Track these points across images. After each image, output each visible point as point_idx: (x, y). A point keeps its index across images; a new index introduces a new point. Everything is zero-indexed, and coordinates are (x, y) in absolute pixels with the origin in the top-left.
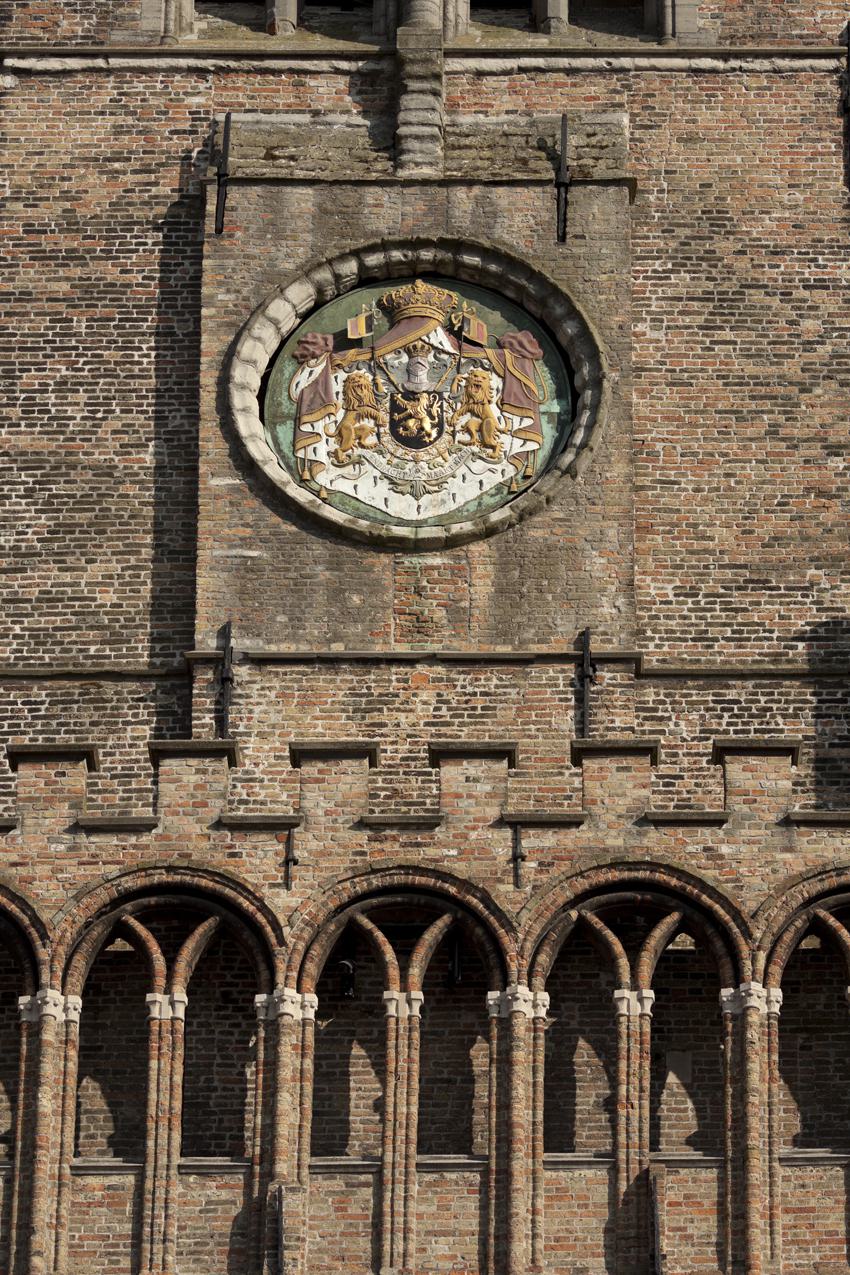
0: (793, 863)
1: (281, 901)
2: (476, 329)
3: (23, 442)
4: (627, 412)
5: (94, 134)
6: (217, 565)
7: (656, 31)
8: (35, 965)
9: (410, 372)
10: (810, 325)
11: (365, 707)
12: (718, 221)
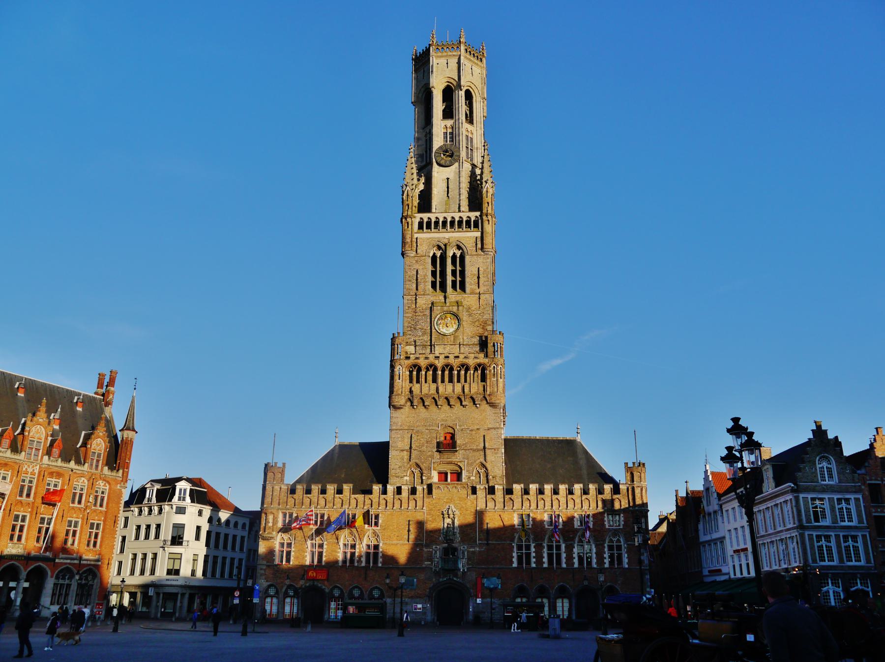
0: (474, 362)
1: (438, 365)
3: (420, 327)
5: (424, 302)
7: (465, 293)
10: (476, 317)
12: (469, 308)
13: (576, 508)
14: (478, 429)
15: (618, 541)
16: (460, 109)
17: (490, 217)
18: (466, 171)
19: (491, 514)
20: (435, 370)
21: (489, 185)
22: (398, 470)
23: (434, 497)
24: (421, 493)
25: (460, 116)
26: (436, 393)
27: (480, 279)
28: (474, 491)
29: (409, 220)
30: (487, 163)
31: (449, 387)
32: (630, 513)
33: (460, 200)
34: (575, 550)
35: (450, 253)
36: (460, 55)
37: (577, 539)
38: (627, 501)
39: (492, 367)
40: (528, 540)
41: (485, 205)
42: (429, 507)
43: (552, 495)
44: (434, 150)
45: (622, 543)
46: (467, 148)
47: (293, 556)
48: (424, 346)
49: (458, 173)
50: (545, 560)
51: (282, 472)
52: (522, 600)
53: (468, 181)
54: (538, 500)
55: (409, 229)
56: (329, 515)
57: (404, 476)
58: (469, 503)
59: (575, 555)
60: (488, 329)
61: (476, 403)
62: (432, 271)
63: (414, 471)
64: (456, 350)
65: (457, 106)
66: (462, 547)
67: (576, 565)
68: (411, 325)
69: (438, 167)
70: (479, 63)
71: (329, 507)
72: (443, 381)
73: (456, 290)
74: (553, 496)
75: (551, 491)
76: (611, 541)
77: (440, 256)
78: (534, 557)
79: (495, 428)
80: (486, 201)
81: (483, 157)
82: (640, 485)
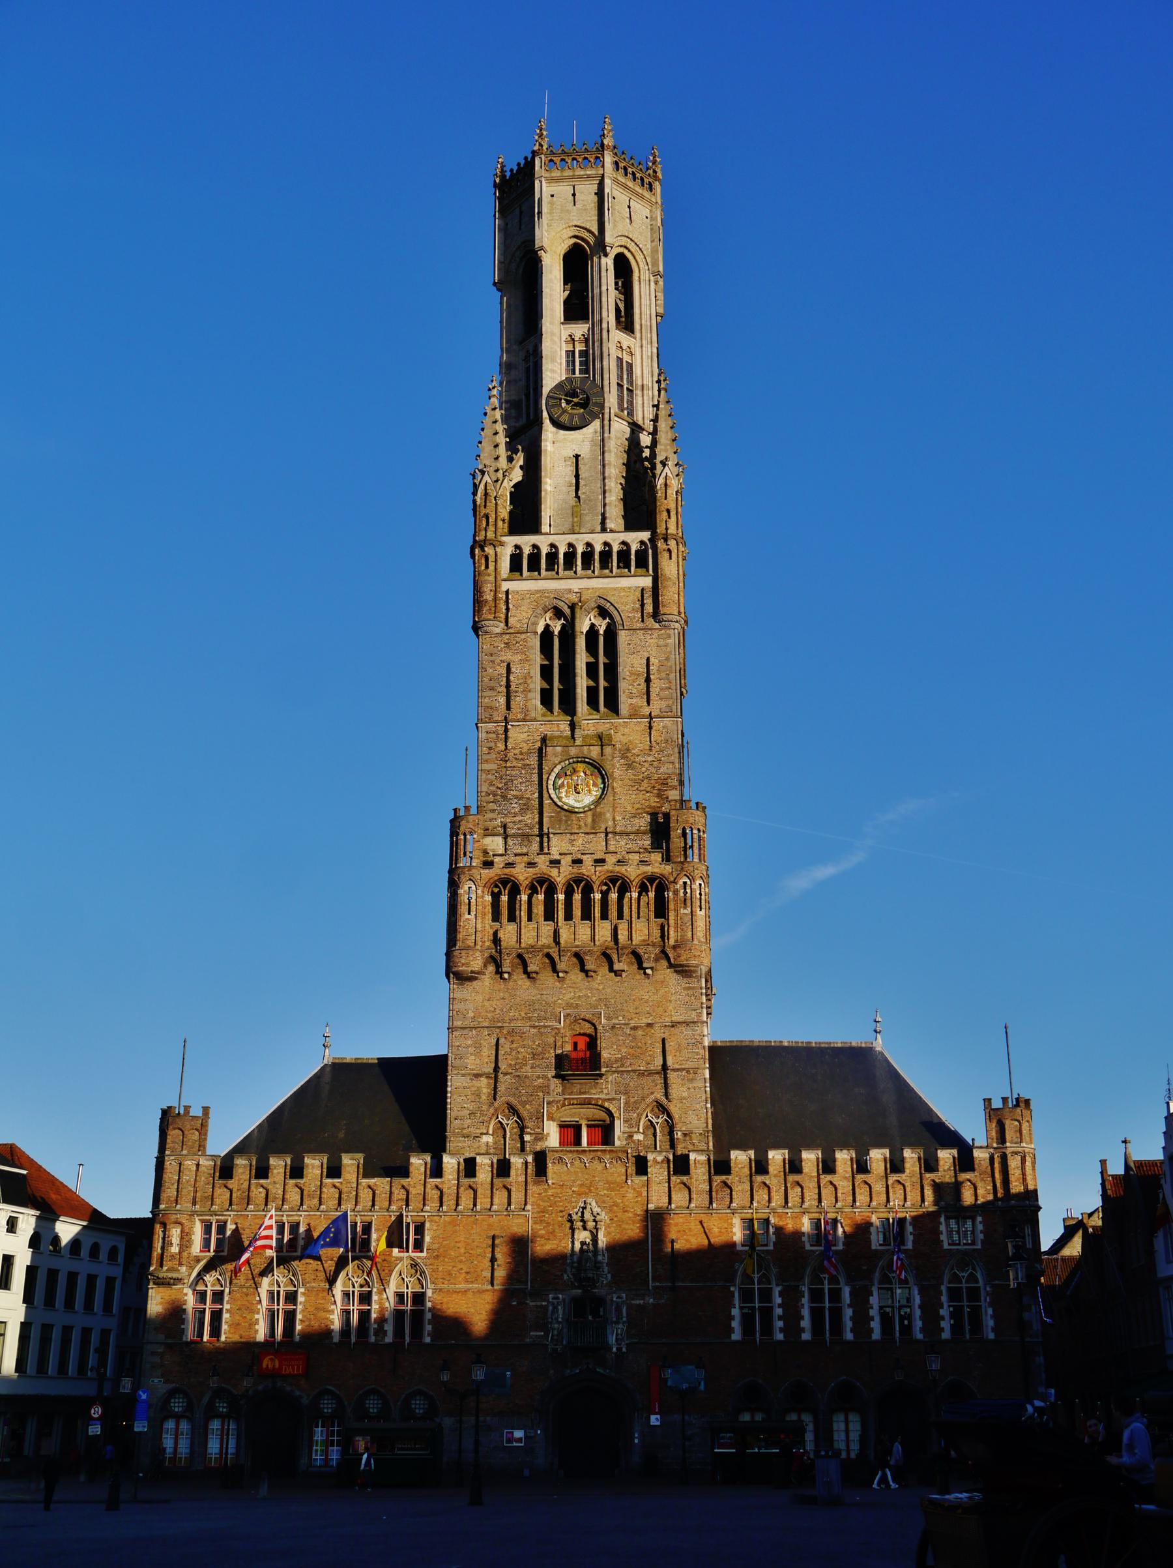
0: (639, 872)
1: (558, 879)
2: (588, 772)
3: (515, 793)
4: (613, 788)
5: (524, 736)
6: (547, 817)
8: (520, 891)
9: (577, 780)
10: (644, 769)
11: (571, 841)
12: (628, 750)
13: (874, 1204)
14: (650, 1025)
15: (972, 1278)
16: (604, 299)
17: (672, 543)
18: (617, 438)
19: (681, 1220)
20: (551, 890)
21: (670, 470)
22: (469, 1121)
23: (550, 1182)
24: (519, 1172)
25: (604, 314)
26: (554, 944)
27: (651, 684)
28: (641, 1166)
29: (489, 550)
30: (665, 421)
31: (584, 930)
33: (605, 505)
34: (874, 1300)
35: (583, 626)
36: (603, 175)
38: (990, 1187)
39: (681, 882)
40: (765, 1279)
41: (662, 516)
42: (539, 1205)
43: (819, 1175)
44: (546, 391)
45: (981, 1284)
46: (620, 386)
47: (226, 1322)
48: (525, 837)
49: (599, 443)
50: (806, 1323)
51: (203, 1129)
52: (753, 1417)
53: (622, 461)
54: (788, 1185)
55: (489, 571)
56: (309, 1225)
57: (482, 1134)
58: (630, 1195)
59: (874, 1312)
60: (670, 798)
61: (645, 965)
62: (541, 665)
63: (505, 1122)
64: (597, 845)
65: (596, 291)
67: (876, 1335)
68: (493, 788)
69: (554, 429)
70: (647, 194)
71: (311, 1209)
72: (568, 917)
73: (598, 710)
74: (822, 1177)
75: (818, 1166)
76: (955, 1278)
77: (560, 633)
78: (780, 1318)
79: (687, 1023)
80: (664, 508)
81: (657, 406)
82: (1020, 1150)
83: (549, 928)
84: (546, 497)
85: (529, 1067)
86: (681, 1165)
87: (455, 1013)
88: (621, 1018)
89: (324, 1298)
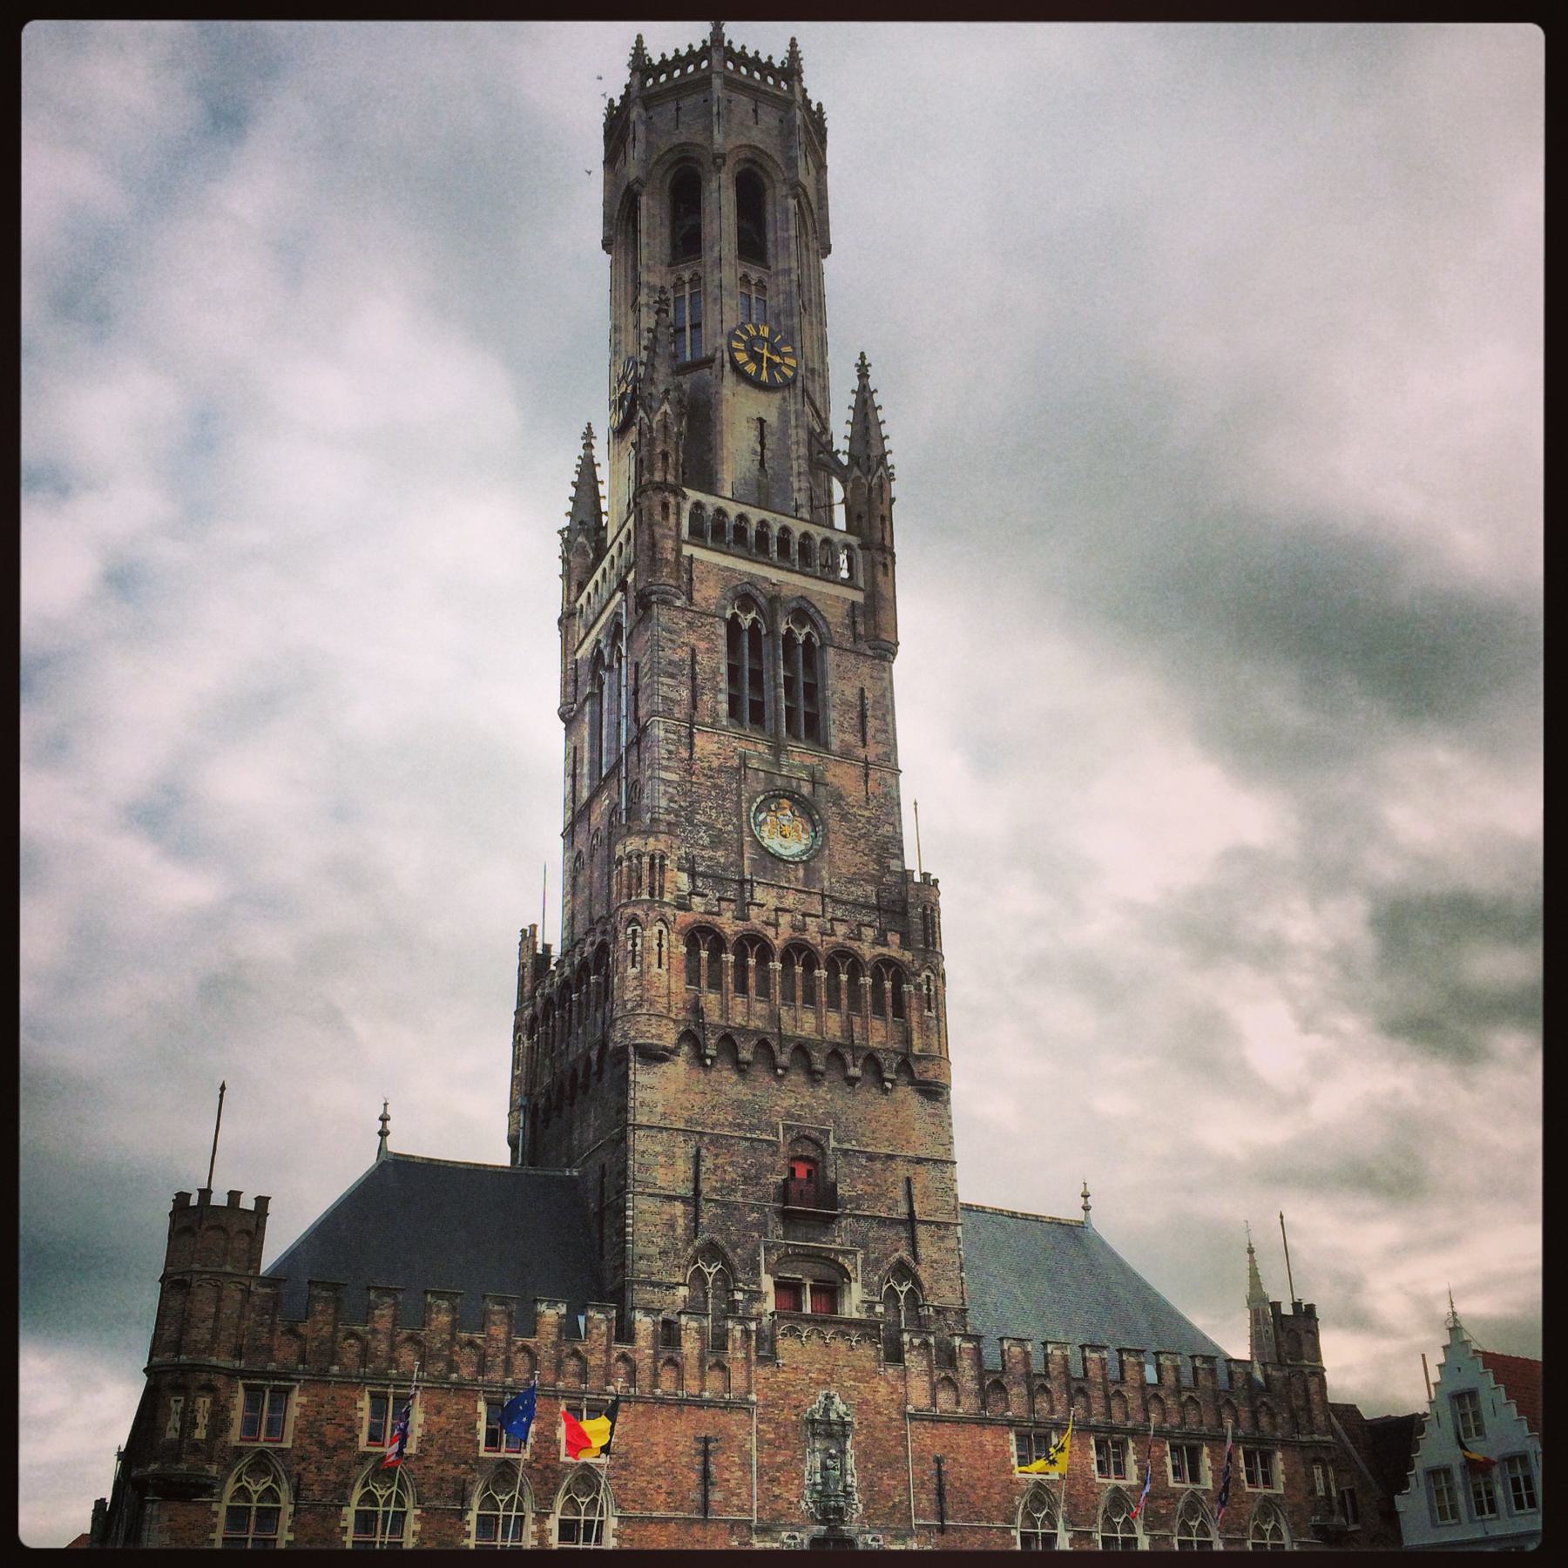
1: (776, 942)
3: (702, 819)
6: (748, 858)
10: (860, 825)
11: (780, 898)
12: (841, 797)
14: (891, 1157)
22: (660, 1263)
28: (895, 1355)
32: (1298, 1449)
35: (783, 629)
37: (1177, 1523)
39: (923, 976)
48: (719, 880)
58: (883, 1389)
60: (892, 868)
66: (869, 1537)
72: (789, 997)
73: (797, 737)
79: (936, 1161)
83: (762, 1005)
84: (727, 458)
85: (739, 1194)
86: (948, 1358)
87: (637, 1104)
88: (854, 1142)
89: (452, 1526)
